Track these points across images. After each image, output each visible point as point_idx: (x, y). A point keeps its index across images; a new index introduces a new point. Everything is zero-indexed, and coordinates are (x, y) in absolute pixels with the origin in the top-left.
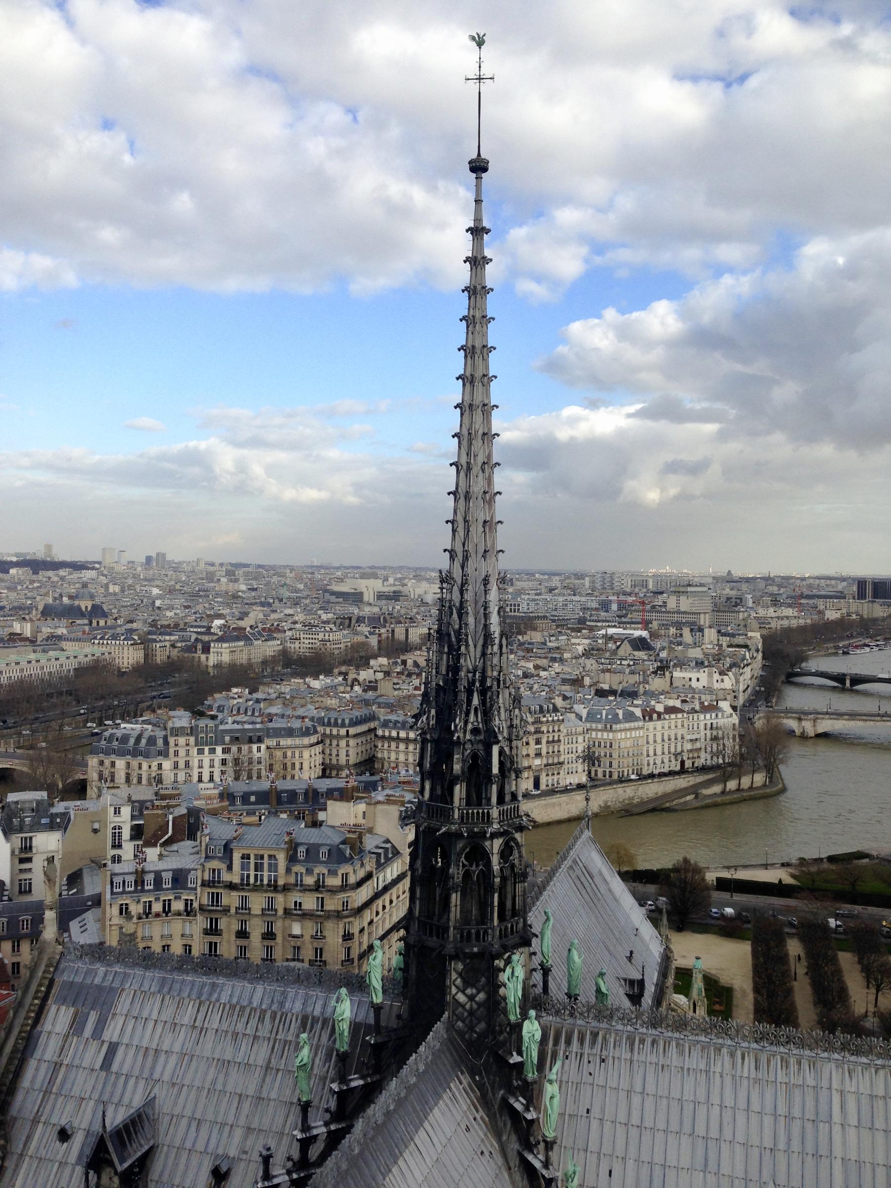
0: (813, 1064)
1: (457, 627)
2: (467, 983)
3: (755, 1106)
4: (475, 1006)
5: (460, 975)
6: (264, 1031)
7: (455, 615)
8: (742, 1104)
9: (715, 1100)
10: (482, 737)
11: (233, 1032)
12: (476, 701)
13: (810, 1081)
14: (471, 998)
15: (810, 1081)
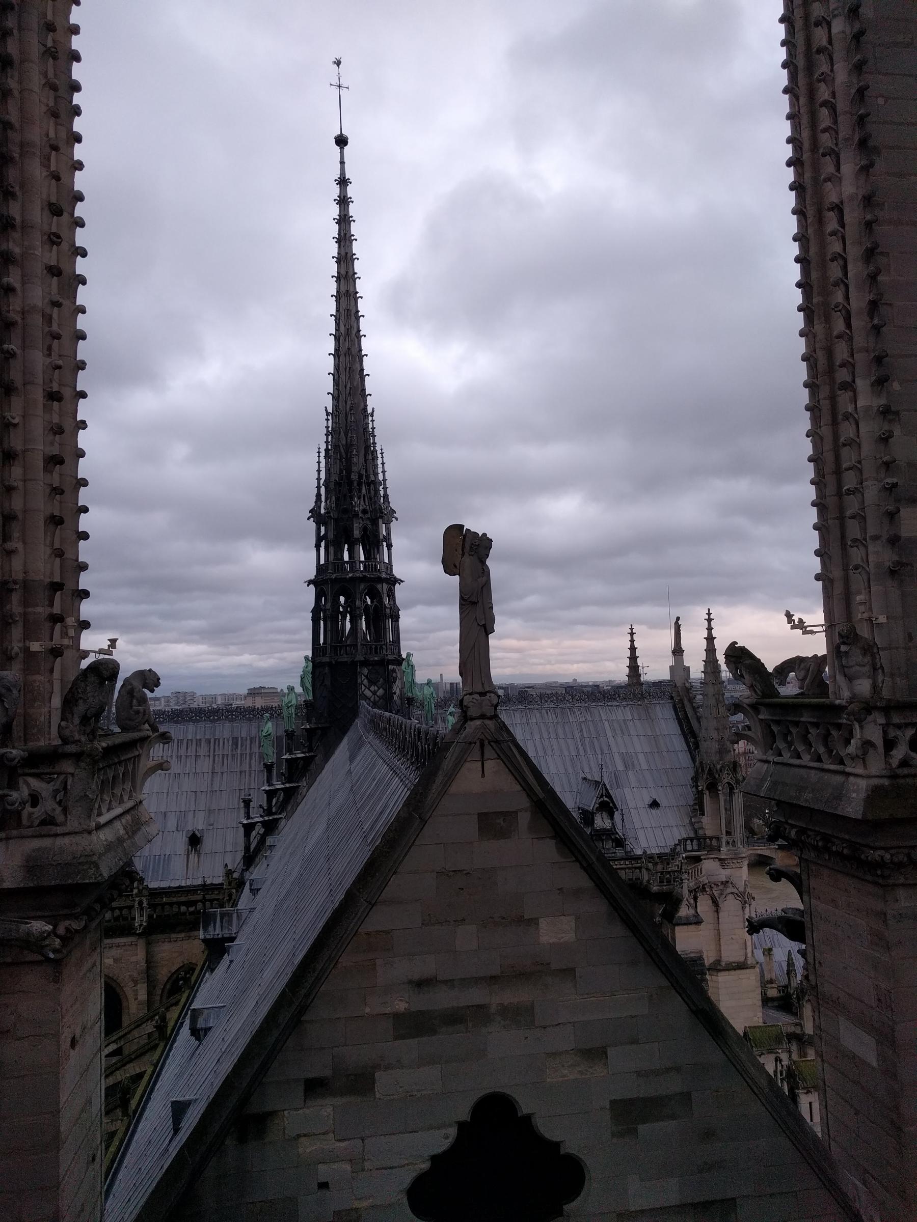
0: (587, 709)
1: (344, 442)
2: (372, 683)
3: (562, 736)
4: (377, 699)
5: (366, 677)
6: (203, 750)
7: (342, 434)
8: (553, 736)
9: (537, 736)
10: (368, 516)
11: (177, 756)
12: (364, 491)
13: (589, 718)
14: (374, 693)
15: (589, 718)
